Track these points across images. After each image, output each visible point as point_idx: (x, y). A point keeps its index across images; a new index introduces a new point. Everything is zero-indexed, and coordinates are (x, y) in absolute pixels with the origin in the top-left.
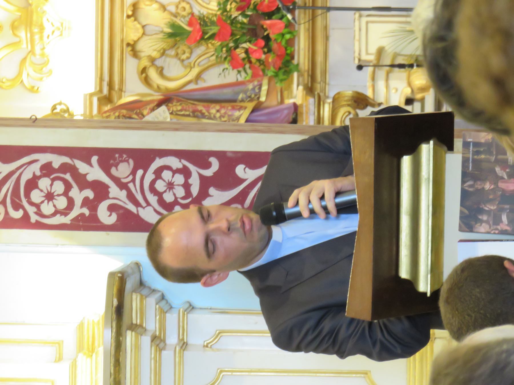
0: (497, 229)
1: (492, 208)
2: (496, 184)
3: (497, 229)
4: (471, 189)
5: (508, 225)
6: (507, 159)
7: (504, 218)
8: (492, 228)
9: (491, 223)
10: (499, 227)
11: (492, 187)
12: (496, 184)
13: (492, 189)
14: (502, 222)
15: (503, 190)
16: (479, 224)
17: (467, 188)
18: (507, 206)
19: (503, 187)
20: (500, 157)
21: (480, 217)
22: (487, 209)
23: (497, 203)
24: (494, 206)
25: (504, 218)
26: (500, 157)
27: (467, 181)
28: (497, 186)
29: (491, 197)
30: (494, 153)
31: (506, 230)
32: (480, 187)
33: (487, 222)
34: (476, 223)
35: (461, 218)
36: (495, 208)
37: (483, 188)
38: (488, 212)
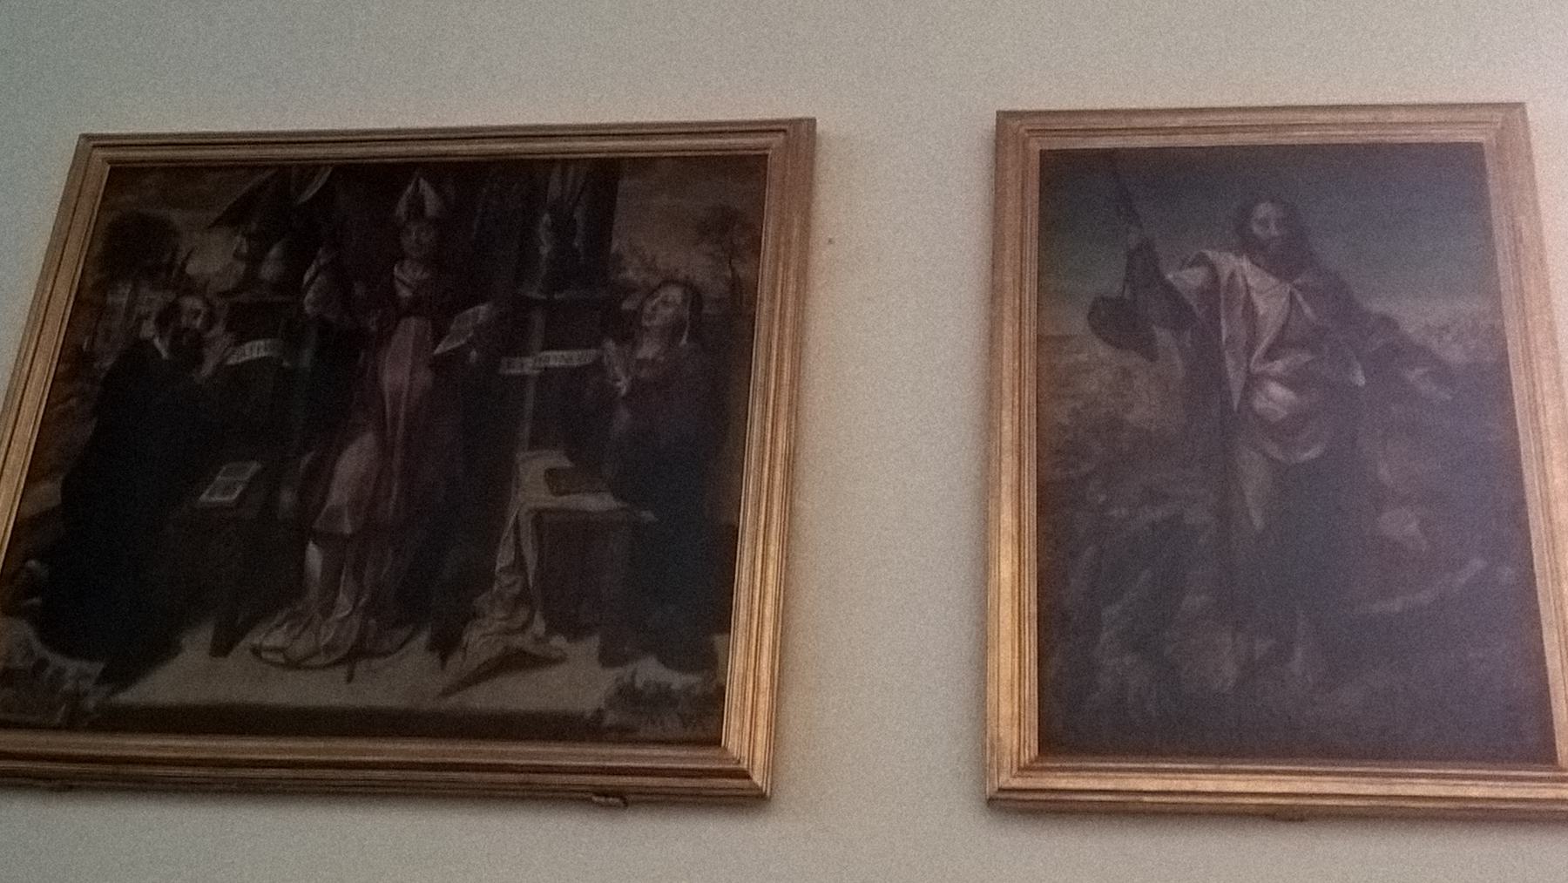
0: (211, 321)
1: (310, 295)
2: (415, 307)
3: (211, 321)
4: (401, 209)
5: (221, 366)
6: (525, 353)
7: (256, 350)
8: (218, 303)
9: (244, 297)
10: (219, 329)
11: (405, 293)
12: (415, 307)
13: (393, 292)
14: (241, 340)
15: (384, 338)
16: (244, 250)
17: (410, 189)
18: (306, 358)
19: (398, 337)
20: (538, 319)
21: (274, 252)
22: (307, 278)
23: (331, 317)
24: (315, 304)
25: (256, 350)
26: (538, 319)
27: (438, 190)
28: (408, 314)
29: (359, 290)
30: (556, 296)
31: (199, 361)
32: (408, 241)
33: (251, 279)
34: (250, 237)
35: (282, 169)
36: (308, 309)
37: (400, 257)
38: (291, 284)
